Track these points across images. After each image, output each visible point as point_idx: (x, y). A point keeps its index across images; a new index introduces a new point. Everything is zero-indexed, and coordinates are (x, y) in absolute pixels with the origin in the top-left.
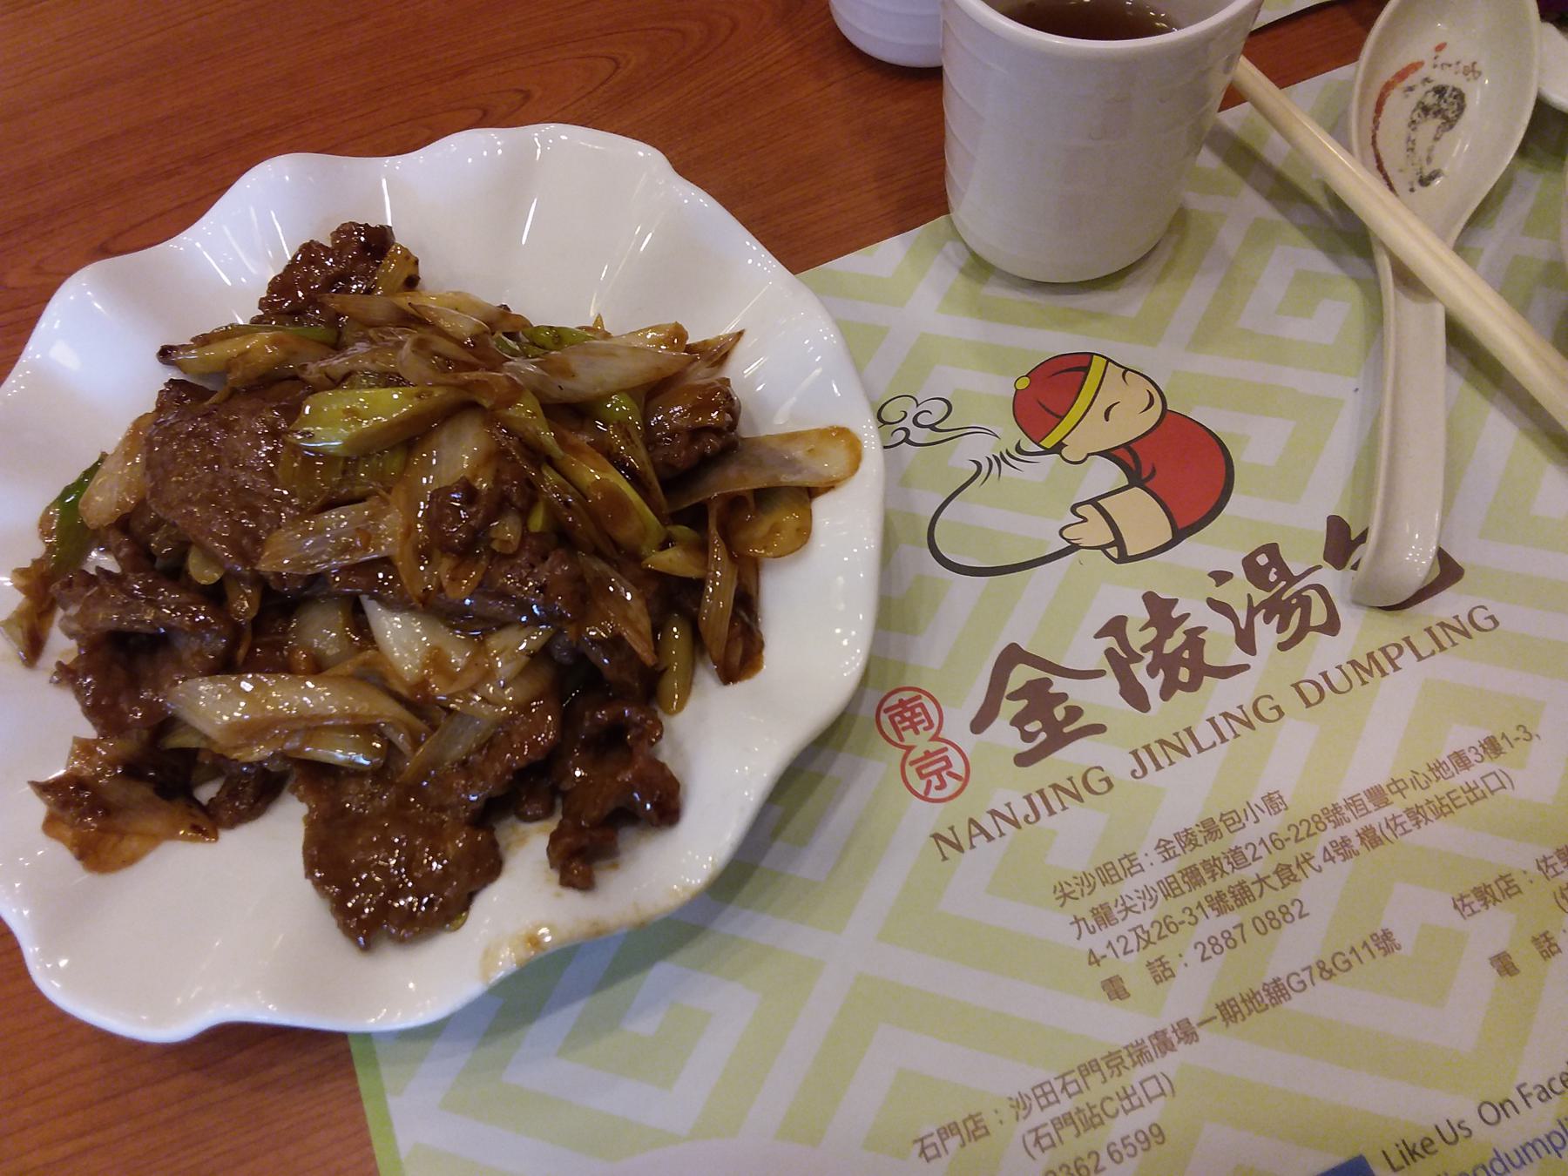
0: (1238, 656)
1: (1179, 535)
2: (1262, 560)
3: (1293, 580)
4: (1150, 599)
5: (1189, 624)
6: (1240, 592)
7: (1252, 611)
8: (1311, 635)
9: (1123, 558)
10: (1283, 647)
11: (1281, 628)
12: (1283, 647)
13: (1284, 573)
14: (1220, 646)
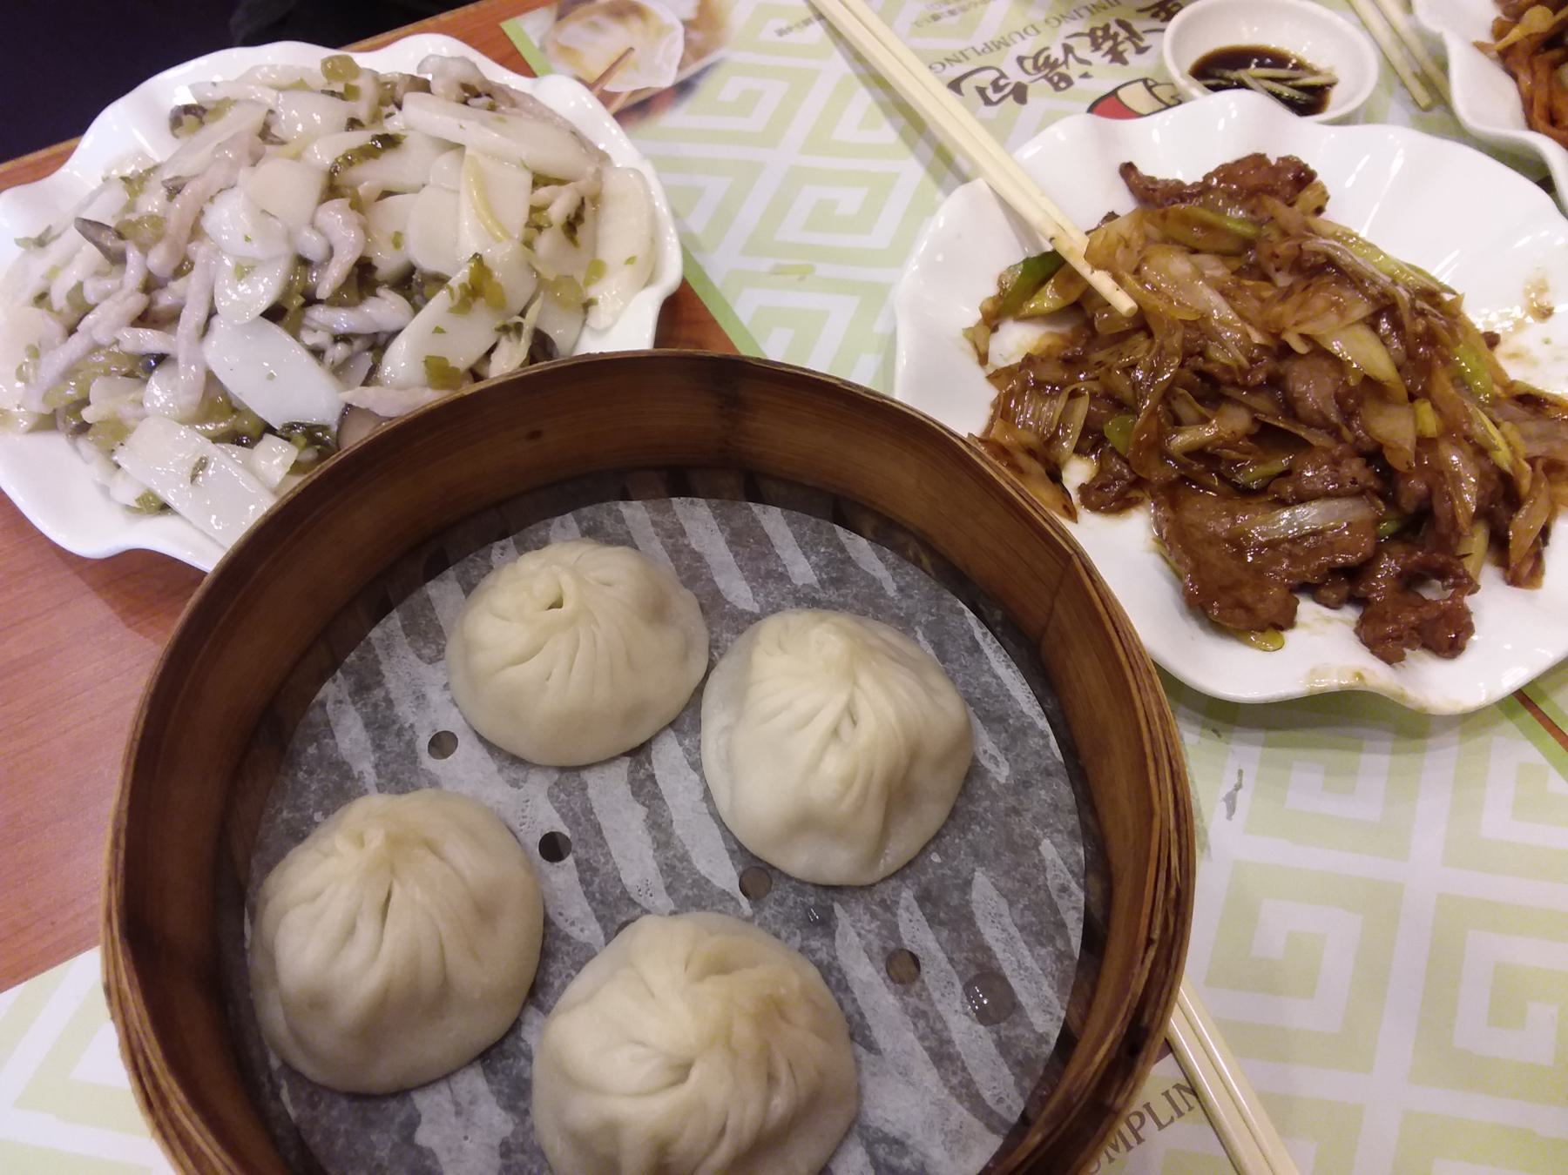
0: (1071, 42)
1: (1114, 93)
2: (1063, 85)
3: (1045, 77)
4: (1125, 62)
5: (1100, 53)
6: (1074, 70)
7: (1066, 62)
8: (1033, 53)
9: (1145, 81)
10: (1047, 49)
11: (1048, 58)
12: (1047, 49)
13: (1050, 80)
14: (1083, 48)
